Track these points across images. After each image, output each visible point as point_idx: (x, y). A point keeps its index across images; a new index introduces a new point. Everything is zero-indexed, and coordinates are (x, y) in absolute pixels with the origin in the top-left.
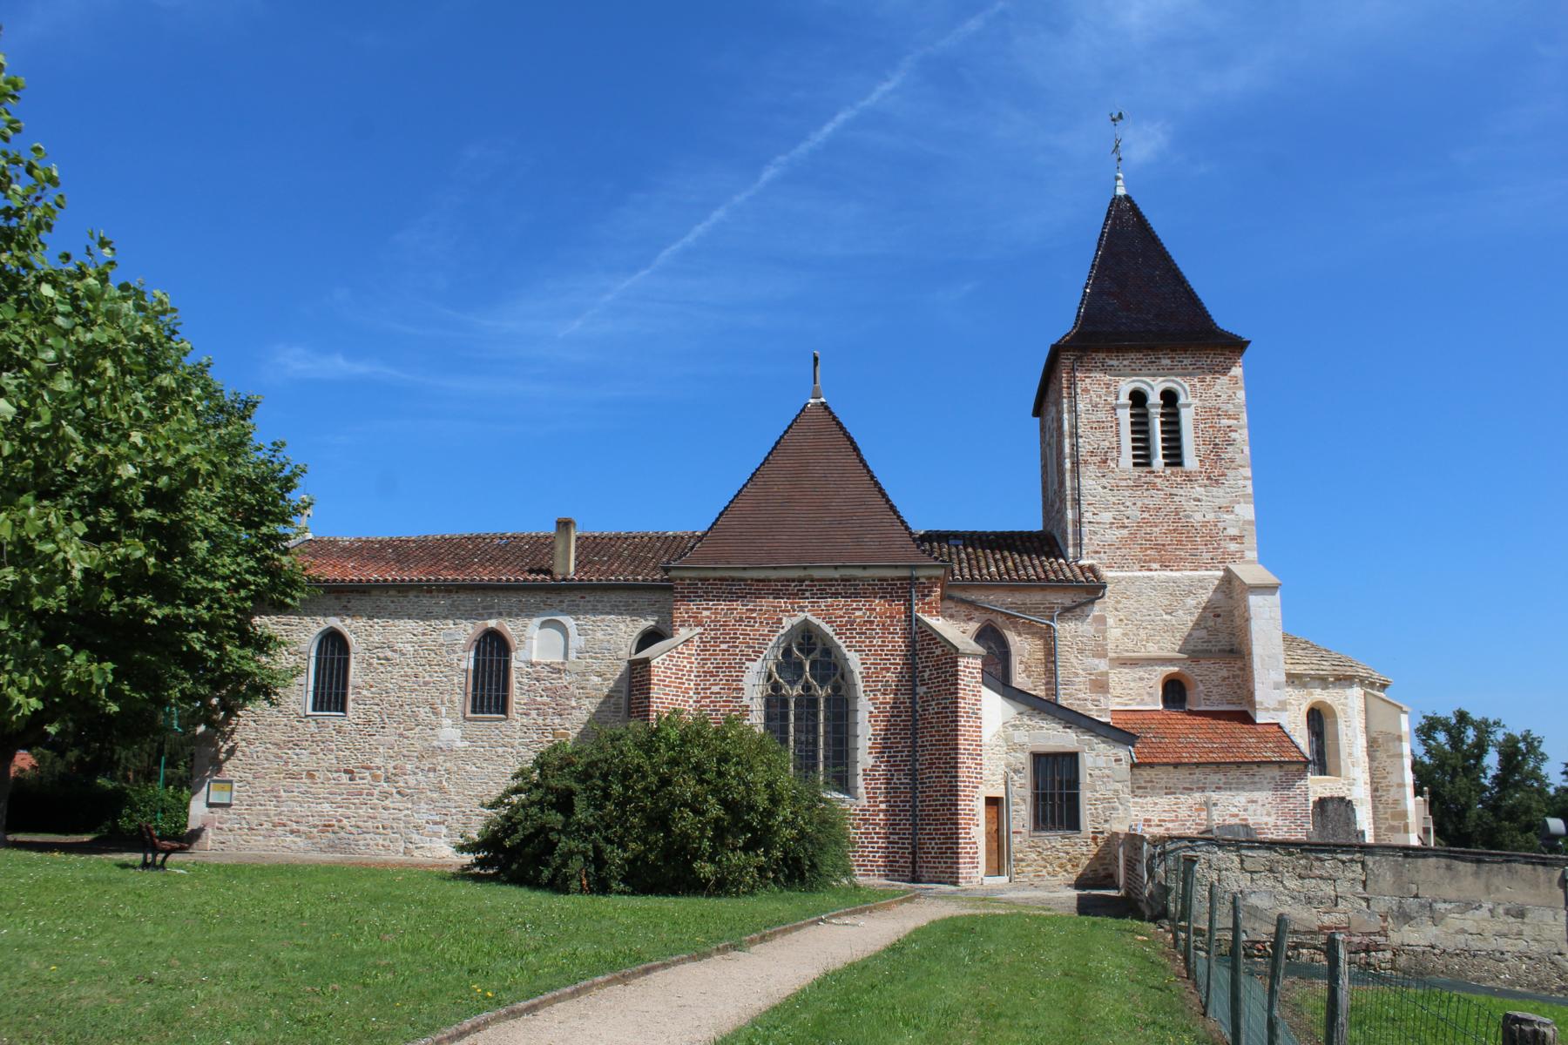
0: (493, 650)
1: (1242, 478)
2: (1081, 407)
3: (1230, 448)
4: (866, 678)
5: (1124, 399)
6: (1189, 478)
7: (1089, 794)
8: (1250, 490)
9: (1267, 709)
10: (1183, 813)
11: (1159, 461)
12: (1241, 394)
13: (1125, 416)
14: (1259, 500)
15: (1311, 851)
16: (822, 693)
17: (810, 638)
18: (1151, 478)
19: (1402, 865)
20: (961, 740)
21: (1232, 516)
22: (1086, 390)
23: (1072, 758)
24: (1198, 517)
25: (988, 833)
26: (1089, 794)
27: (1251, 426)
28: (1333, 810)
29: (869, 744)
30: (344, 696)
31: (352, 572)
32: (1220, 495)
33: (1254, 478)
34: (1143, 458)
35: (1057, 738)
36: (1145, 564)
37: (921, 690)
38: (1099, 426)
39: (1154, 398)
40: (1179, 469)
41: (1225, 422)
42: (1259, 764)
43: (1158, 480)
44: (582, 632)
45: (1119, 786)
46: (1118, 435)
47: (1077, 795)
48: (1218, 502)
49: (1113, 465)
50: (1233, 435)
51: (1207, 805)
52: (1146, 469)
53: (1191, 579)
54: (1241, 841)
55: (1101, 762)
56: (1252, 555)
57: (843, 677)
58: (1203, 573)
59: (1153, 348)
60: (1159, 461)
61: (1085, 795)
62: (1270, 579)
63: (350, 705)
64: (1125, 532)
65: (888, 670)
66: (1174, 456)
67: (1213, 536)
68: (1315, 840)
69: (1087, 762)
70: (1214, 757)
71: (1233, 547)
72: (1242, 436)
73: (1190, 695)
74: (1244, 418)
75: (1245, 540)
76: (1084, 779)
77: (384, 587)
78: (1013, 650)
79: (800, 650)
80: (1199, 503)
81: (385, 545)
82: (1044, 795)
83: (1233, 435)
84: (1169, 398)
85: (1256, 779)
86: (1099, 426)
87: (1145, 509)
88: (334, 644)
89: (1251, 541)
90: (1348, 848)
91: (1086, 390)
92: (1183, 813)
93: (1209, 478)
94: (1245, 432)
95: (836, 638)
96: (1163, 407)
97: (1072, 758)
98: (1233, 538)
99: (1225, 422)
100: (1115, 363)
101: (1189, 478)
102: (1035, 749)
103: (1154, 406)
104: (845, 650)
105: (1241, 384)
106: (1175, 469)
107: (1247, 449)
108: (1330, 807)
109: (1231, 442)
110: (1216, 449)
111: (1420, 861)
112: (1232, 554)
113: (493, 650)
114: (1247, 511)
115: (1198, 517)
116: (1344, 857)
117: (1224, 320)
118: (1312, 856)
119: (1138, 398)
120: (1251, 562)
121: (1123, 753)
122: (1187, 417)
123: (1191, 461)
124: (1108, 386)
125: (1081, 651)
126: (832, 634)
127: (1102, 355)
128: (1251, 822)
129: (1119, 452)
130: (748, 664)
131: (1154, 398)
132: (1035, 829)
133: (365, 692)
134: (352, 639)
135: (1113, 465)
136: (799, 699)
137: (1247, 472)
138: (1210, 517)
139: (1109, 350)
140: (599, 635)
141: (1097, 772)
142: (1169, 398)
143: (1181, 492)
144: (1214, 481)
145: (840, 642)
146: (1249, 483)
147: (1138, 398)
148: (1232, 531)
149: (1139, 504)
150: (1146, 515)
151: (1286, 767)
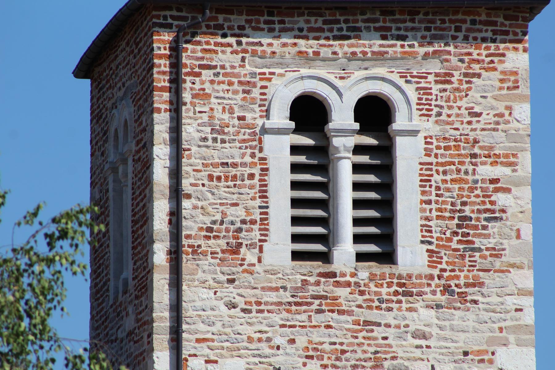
1: (514, 291)
3: (494, 228)
5: (281, 117)
6: (406, 289)
8: (529, 317)
12: (523, 112)
13: (279, 152)
18: (326, 287)
22: (202, 95)
27: (538, 181)
32: (466, 326)
33: (537, 293)
38: (225, 174)
39: (342, 116)
41: (486, 171)
43: (343, 292)
46: (263, 195)
48: (463, 341)
50: (501, 199)
72: (517, 202)
74: (526, 161)
83: (501, 199)
86: (225, 174)
91: (202, 95)
93: (447, 290)
94: (525, 194)
99: (486, 171)
101: (406, 289)
105: (524, 89)
107: (527, 231)
109: (495, 215)
110: (465, 227)
119: (309, 113)
122: (408, 155)
124: (247, 86)
129: (265, 231)
131: (342, 116)
135: (251, 257)
137: (525, 279)
142: (374, 113)
143: (388, 317)
144: (456, 295)
146: (528, 302)
147: (309, 113)
149: (302, 341)
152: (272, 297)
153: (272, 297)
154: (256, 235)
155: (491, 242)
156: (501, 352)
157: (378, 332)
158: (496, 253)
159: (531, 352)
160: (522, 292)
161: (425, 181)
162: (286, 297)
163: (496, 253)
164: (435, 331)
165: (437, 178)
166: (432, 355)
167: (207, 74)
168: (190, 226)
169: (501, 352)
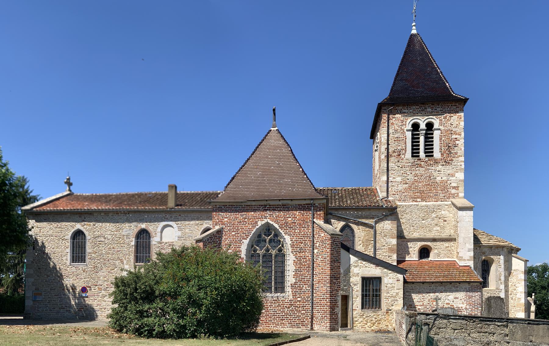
0: (143, 237)
2: (391, 131)
3: (456, 148)
4: (292, 246)
5: (409, 127)
7: (385, 294)
8: (463, 167)
9: (465, 260)
10: (426, 303)
11: (422, 154)
13: (409, 135)
14: (466, 171)
15: (483, 321)
16: (274, 252)
17: (269, 230)
18: (418, 162)
19: (527, 328)
20: (328, 272)
21: (454, 178)
23: (378, 280)
24: (439, 179)
25: (342, 310)
26: (385, 294)
28: (497, 304)
29: (294, 273)
30: (85, 257)
31: (86, 206)
32: (448, 169)
34: (415, 153)
35: (373, 271)
36: (414, 199)
37: (316, 251)
39: (423, 126)
40: (432, 158)
42: (460, 282)
44: (180, 229)
45: (397, 291)
47: (380, 295)
49: (403, 157)
51: (437, 299)
52: (418, 158)
53: (435, 206)
54: (452, 316)
55: (391, 281)
56: (462, 195)
57: (283, 246)
58: (439, 203)
59: (423, 104)
60: (422, 154)
61: (384, 295)
62: (467, 203)
63: (87, 260)
64: (407, 185)
65: (302, 243)
66: (429, 152)
67: (445, 187)
68: (485, 315)
69: (385, 281)
70: (441, 280)
71: (453, 191)
73: (431, 254)
75: (460, 188)
76: (383, 288)
77: (99, 212)
78: (356, 235)
79: (265, 235)
80: (440, 173)
81: (101, 196)
82: (366, 295)
83: (457, 142)
84: (430, 126)
85: (458, 289)
86: (397, 140)
87: (416, 175)
88: (78, 235)
89: (462, 189)
90: (500, 320)
91: (393, 124)
92: (426, 303)
93: (445, 161)
95: (280, 230)
96: (426, 130)
97: (378, 280)
98: (454, 188)
100: (406, 111)
101: (436, 162)
102: (363, 276)
103: (422, 130)
104: (284, 235)
106: (430, 158)
108: (492, 301)
110: (449, 149)
111: (535, 326)
112: (454, 194)
113: (143, 237)
114: (461, 176)
115: (439, 179)
116: (499, 324)
117: (457, 91)
118: (483, 323)
119: (416, 127)
120: (461, 198)
121: (401, 277)
122: (436, 135)
123: (437, 154)
124: (402, 121)
125: (385, 236)
126: (278, 228)
127: (400, 108)
128: (455, 306)
129: (406, 151)
130: (243, 240)
131: (423, 126)
132: (362, 308)
133: (93, 255)
134: (86, 233)
135: (403, 157)
136: (264, 256)
137: (462, 159)
138: (445, 178)
139: (404, 105)
140: (187, 231)
141: (389, 285)
142: (430, 126)
143: (433, 168)
144: (447, 163)
145: (281, 231)
147: (416, 127)
148: (454, 185)
149: (413, 173)
150: (416, 178)
151: (471, 284)
152: (407, 165)
153: (407, 165)
154: (404, 152)
155: (455, 151)
156: (456, 174)
157: (430, 171)
158: (456, 153)
159: (463, 174)
160: (461, 161)
161: (441, 139)
162: (410, 164)
163: (456, 153)
164: (442, 170)
165: (443, 138)
166: (442, 175)
167: (394, 119)
168: (390, 151)
169: (456, 174)
